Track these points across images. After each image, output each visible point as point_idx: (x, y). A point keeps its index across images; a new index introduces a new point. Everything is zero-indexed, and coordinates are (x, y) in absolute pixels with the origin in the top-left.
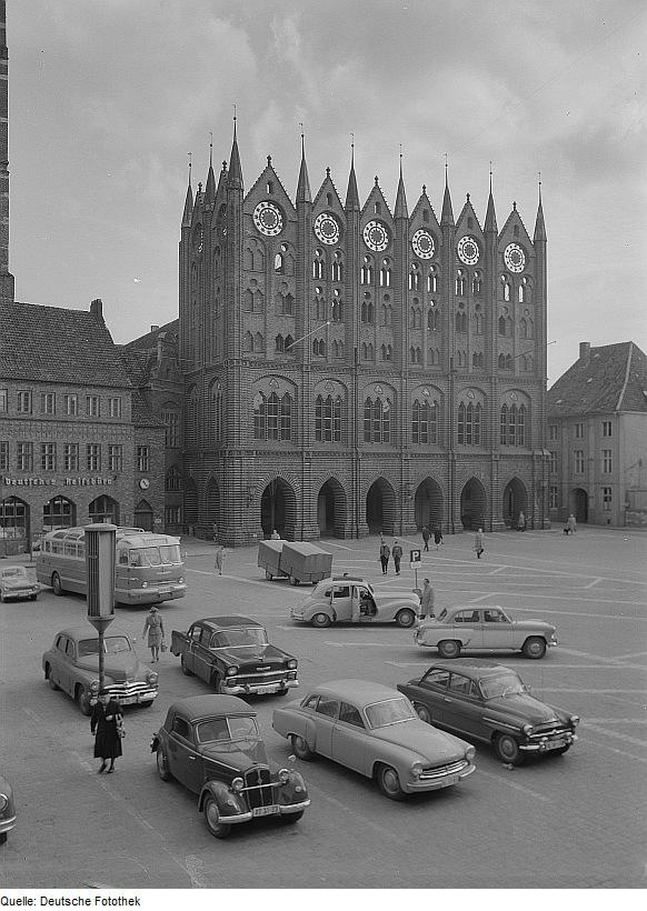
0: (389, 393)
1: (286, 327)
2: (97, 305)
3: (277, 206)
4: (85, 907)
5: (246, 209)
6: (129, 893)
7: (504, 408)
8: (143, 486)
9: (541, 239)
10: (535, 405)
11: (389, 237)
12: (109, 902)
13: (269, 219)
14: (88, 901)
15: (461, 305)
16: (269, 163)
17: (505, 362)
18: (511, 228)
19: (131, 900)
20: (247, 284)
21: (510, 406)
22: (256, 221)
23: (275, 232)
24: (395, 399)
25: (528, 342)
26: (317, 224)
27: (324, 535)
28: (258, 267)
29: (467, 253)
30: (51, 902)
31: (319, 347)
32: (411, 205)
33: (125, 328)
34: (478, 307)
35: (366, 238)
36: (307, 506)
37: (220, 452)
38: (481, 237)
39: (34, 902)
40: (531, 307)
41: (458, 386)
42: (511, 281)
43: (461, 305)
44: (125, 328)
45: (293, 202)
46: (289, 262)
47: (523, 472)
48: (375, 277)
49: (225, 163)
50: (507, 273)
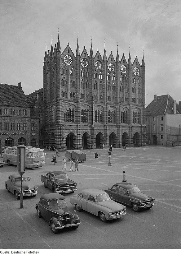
0: (102, 109)
1: (74, 90)
2: (20, 84)
3: (70, 56)
4: (24, 254)
5: (62, 57)
6: (36, 250)
7: (134, 113)
8: (33, 135)
9: (143, 67)
10: (142, 112)
11: (102, 65)
12: (30, 252)
13: (68, 60)
14: (25, 252)
15: (122, 84)
17: (134, 100)
19: (37, 252)
20: (62, 78)
21: (135, 112)
22: (65, 61)
23: (70, 64)
24: (104, 110)
25: (140, 95)
26: (82, 61)
27: (84, 148)
28: (65, 73)
29: (123, 70)
30: (14, 252)
31: (82, 96)
32: (108, 56)
33: (28, 90)
34: (126, 85)
35: (95, 65)
36: (80, 141)
37: (55, 125)
39: (10, 253)
40: (141, 85)
41: (121, 106)
43: (122, 84)
44: (28, 90)
45: (75, 55)
46: (74, 72)
47: (138, 131)
48: (98, 76)
49: (56, 44)
50: (134, 75)
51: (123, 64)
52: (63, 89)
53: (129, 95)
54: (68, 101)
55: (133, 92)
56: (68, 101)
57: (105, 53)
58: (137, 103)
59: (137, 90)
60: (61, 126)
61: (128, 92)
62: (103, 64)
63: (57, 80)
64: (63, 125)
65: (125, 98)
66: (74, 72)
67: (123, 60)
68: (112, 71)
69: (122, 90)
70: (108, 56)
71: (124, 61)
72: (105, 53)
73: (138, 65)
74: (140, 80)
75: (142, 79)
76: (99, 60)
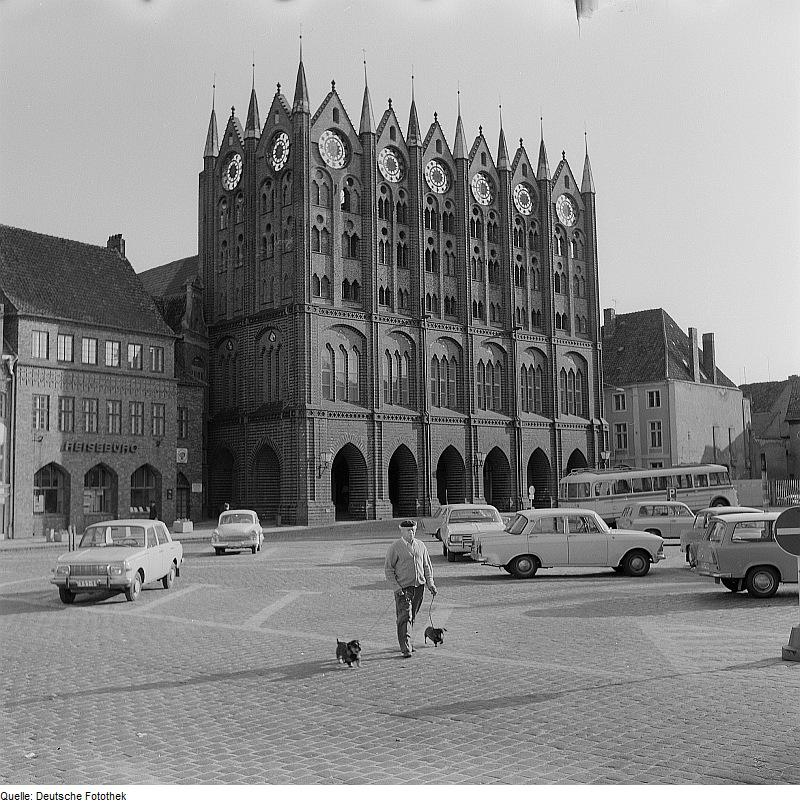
16: (333, 87)
17: (563, 322)
18: (561, 179)
20: (314, 222)
23: (334, 164)
24: (461, 357)
33: (143, 258)
37: (290, 411)
40: (582, 264)
51: (524, 179)
52: (318, 265)
53: (546, 302)
54: (335, 312)
55: (558, 290)
57: (459, 131)
60: (316, 414)
61: (542, 288)
63: (297, 225)
65: (533, 313)
66: (354, 198)
67: (520, 166)
68: (441, 192)
71: (568, 180)
72: (459, 131)
73: (572, 185)
74: (579, 246)
75: (587, 241)
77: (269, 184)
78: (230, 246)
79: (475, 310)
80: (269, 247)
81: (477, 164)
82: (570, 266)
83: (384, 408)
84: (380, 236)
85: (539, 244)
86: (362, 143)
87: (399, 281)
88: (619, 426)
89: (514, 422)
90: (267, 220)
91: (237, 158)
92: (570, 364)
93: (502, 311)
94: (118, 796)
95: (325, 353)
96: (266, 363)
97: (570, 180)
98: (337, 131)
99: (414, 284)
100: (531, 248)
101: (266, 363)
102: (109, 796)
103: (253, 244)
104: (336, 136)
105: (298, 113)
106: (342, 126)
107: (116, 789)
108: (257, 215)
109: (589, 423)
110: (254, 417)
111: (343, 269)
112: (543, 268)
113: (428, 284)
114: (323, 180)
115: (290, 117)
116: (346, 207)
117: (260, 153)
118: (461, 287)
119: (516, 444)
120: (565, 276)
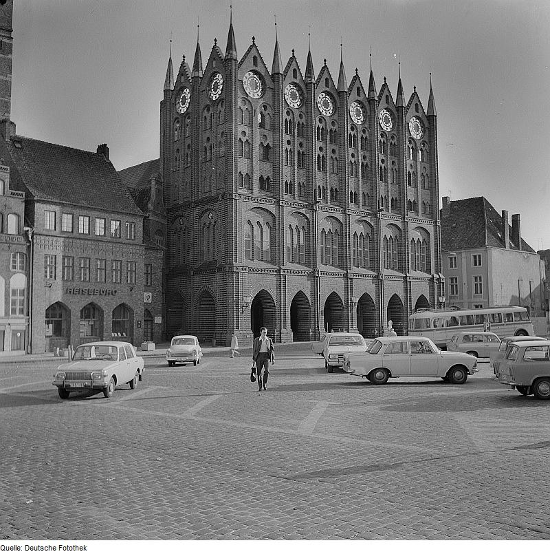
15: (383, 161)
16: (253, 42)
17: (413, 206)
18: (413, 106)
20: (239, 136)
23: (254, 96)
34: (393, 163)
37: (222, 267)
38: (394, 110)
40: (427, 166)
42: (414, 145)
44: (121, 161)
51: (386, 106)
52: (242, 166)
53: (402, 192)
54: (254, 199)
55: (410, 184)
56: (254, 199)
57: (341, 72)
58: (420, 216)
59: (419, 179)
60: (240, 270)
61: (399, 183)
62: (338, 101)
63: (228, 138)
64: (244, 268)
65: (392, 199)
66: (267, 119)
68: (328, 115)
69: (384, 178)
70: (317, 72)
71: (418, 106)
72: (341, 72)
73: (420, 111)
74: (425, 153)
75: (430, 149)
76: (328, 89)
77: (208, 110)
78: (181, 153)
79: (352, 198)
80: (208, 153)
81: (354, 95)
82: (419, 166)
83: (288, 265)
84: (286, 146)
85: (396, 151)
86: (273, 81)
87: (299, 177)
88: (452, 279)
89: (378, 276)
90: (207, 134)
91: (187, 91)
92: (416, 235)
93: (370, 198)
94: (81, 547)
95: (247, 227)
96: (206, 233)
97: (419, 107)
98: (256, 72)
99: (309, 179)
100: (392, 154)
101: (206, 233)
102: (75, 548)
103: (197, 151)
104: (255, 76)
105: (229, 59)
106: (259, 68)
107: (79, 543)
108: (200, 131)
109: (431, 277)
110: (198, 272)
111: (260, 169)
112: (399, 168)
113: (319, 179)
114: (246, 107)
115: (223, 63)
116: (262, 125)
117: (202, 88)
118: (342, 181)
119: (379, 291)
120: (415, 174)
